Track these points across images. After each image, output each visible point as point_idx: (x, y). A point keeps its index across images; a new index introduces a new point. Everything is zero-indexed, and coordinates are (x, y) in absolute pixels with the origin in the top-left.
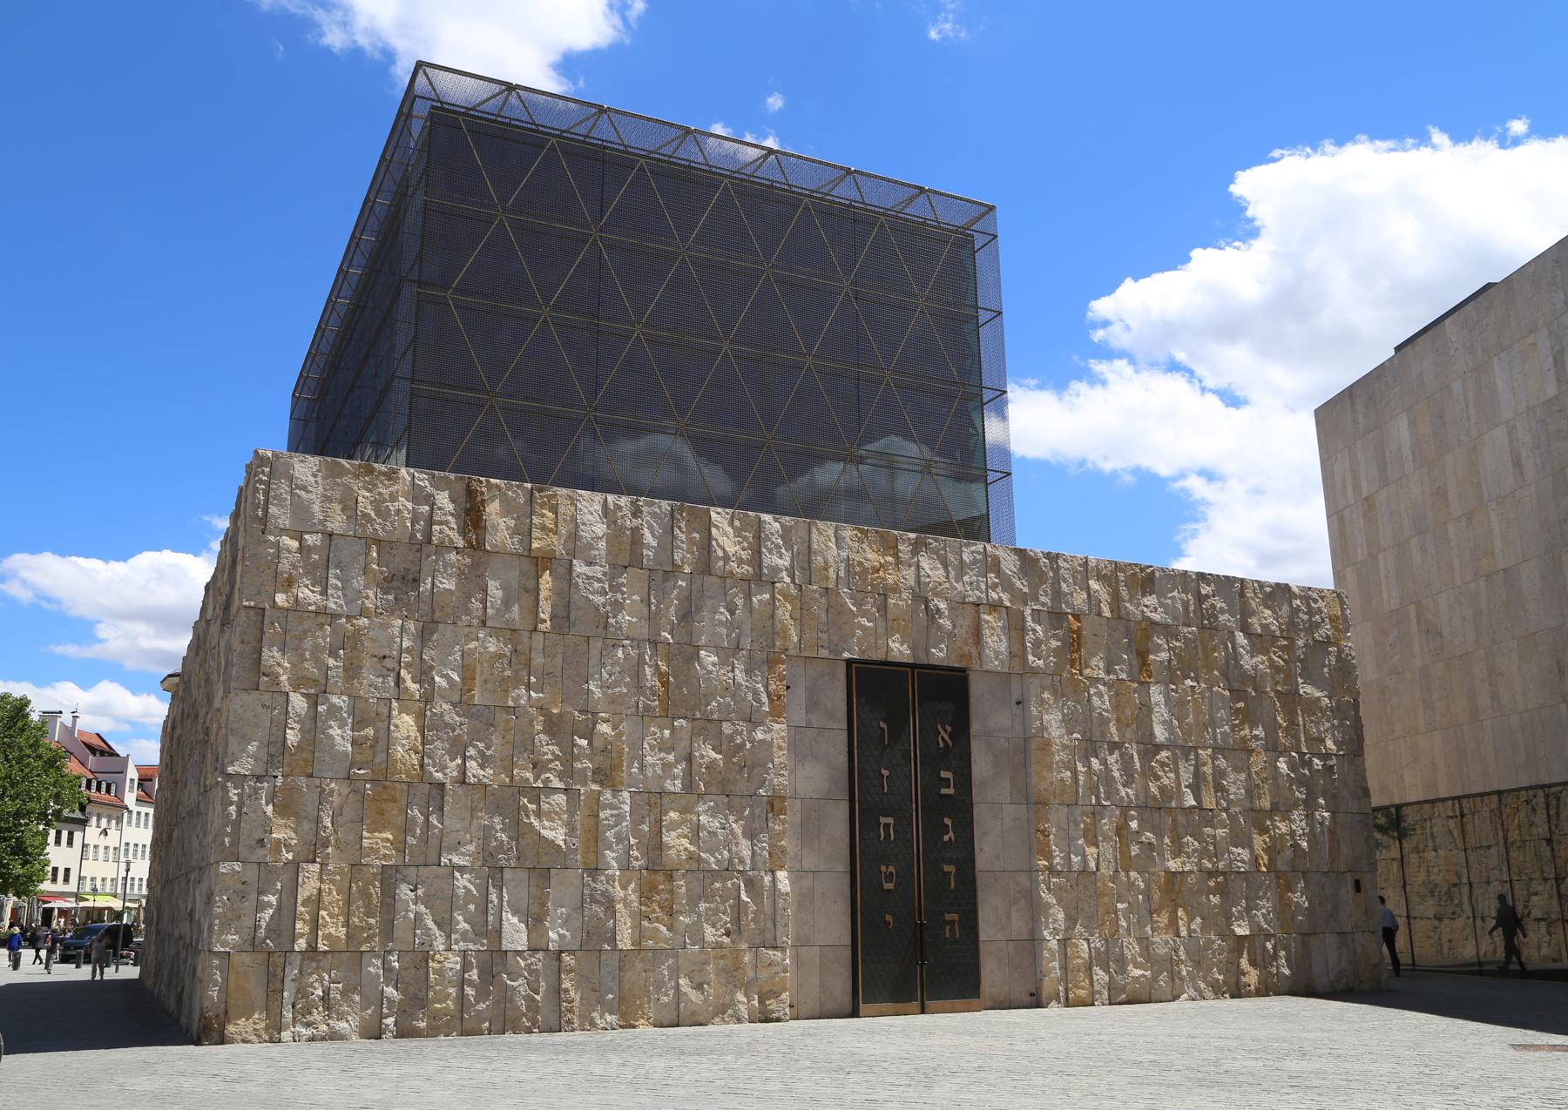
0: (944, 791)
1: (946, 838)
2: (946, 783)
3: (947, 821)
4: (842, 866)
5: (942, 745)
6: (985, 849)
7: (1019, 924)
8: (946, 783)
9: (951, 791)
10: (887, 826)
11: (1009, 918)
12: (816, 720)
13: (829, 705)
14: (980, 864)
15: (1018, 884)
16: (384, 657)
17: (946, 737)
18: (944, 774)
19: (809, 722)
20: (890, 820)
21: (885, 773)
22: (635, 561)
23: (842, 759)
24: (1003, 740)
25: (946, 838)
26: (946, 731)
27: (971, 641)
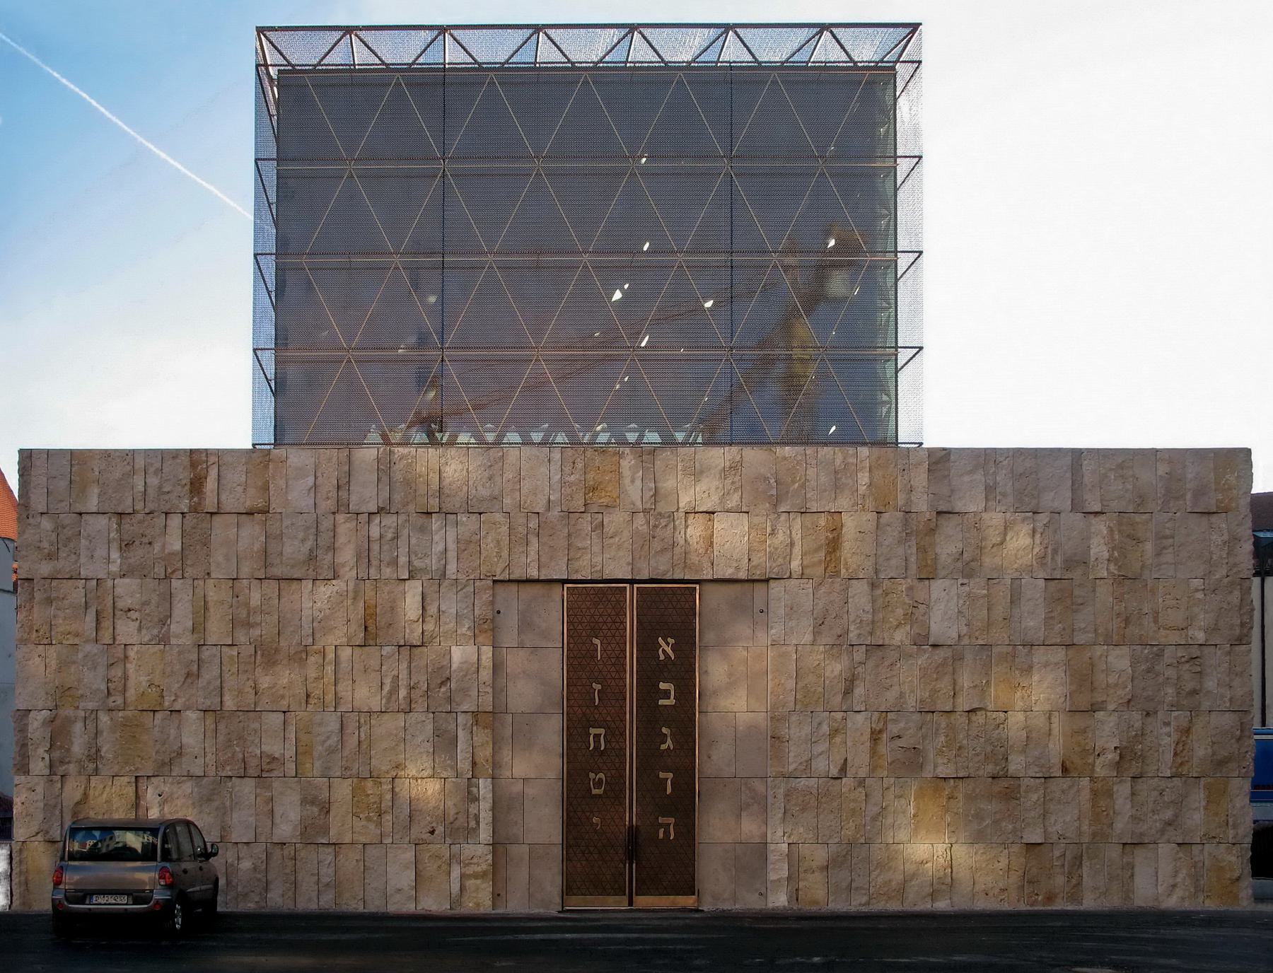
0: (661, 702)
1: (663, 747)
2: (666, 694)
3: (664, 730)
5: (662, 657)
6: (714, 757)
8: (666, 694)
9: (671, 701)
10: (597, 736)
16: (130, 610)
17: (669, 650)
18: (663, 686)
20: (602, 731)
21: (597, 687)
22: (341, 506)
24: (741, 649)
25: (663, 747)
26: (668, 644)
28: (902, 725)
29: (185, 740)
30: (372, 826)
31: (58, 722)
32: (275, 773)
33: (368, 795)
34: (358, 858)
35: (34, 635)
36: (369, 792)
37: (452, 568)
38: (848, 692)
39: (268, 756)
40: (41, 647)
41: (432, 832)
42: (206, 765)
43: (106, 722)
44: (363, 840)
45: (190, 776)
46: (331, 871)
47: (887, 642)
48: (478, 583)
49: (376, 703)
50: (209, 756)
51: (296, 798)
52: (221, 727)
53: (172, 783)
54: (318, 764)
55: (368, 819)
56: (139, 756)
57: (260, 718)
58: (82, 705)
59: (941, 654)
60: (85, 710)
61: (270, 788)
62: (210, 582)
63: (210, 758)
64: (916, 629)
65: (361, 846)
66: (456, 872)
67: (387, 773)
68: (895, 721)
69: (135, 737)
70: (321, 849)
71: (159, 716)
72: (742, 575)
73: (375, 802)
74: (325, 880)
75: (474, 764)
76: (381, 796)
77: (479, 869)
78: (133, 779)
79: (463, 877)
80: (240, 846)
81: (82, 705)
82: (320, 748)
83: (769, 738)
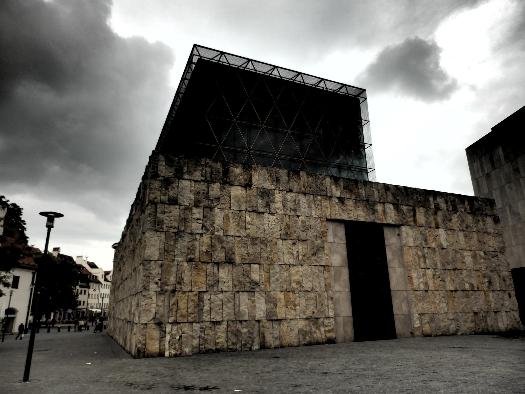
4: (348, 289)
7: (405, 308)
11: (401, 307)
12: (337, 240)
13: (340, 235)
14: (392, 289)
15: (403, 295)
19: (334, 241)
23: (344, 252)
27: (382, 214)
28: (439, 273)
29: (220, 275)
30: (293, 311)
31: (164, 267)
32: (257, 289)
33: (290, 298)
34: (288, 325)
35: (157, 227)
36: (291, 297)
37: (313, 213)
38: (425, 262)
39: (254, 282)
40: (158, 233)
41: (314, 312)
42: (228, 286)
43: (186, 267)
44: (290, 317)
45: (222, 291)
46: (277, 332)
47: (431, 247)
48: (322, 219)
49: (292, 261)
50: (230, 282)
51: (263, 300)
52: (235, 270)
53: (214, 295)
54: (273, 285)
55: (291, 308)
56: (200, 282)
57: (250, 266)
58: (176, 259)
59: (445, 250)
60: (177, 261)
61: (254, 296)
62: (231, 211)
63: (230, 284)
64: (437, 243)
65: (289, 320)
66: (322, 329)
67: (297, 289)
68: (438, 272)
69: (199, 273)
70: (274, 322)
71: (210, 264)
72: (393, 223)
73: (293, 302)
74: (276, 336)
75: (325, 285)
76: (295, 299)
77: (330, 328)
78: (197, 293)
79: (325, 331)
80: (243, 322)
81: (176, 259)
82: (273, 279)
83: (407, 277)
